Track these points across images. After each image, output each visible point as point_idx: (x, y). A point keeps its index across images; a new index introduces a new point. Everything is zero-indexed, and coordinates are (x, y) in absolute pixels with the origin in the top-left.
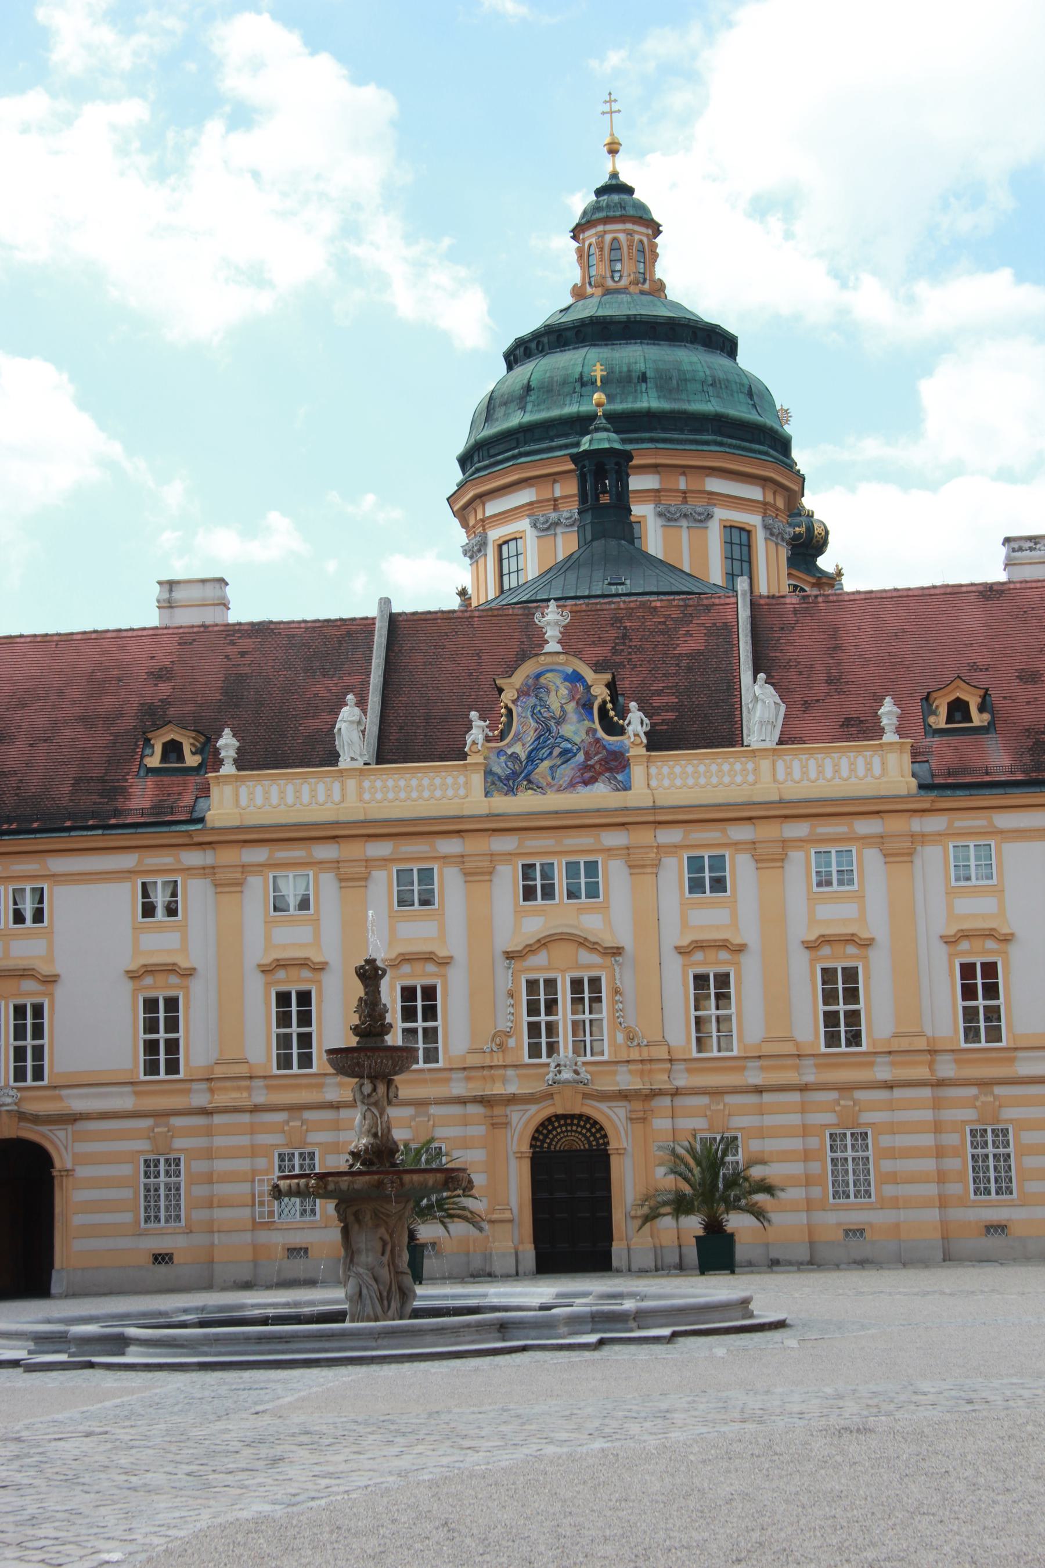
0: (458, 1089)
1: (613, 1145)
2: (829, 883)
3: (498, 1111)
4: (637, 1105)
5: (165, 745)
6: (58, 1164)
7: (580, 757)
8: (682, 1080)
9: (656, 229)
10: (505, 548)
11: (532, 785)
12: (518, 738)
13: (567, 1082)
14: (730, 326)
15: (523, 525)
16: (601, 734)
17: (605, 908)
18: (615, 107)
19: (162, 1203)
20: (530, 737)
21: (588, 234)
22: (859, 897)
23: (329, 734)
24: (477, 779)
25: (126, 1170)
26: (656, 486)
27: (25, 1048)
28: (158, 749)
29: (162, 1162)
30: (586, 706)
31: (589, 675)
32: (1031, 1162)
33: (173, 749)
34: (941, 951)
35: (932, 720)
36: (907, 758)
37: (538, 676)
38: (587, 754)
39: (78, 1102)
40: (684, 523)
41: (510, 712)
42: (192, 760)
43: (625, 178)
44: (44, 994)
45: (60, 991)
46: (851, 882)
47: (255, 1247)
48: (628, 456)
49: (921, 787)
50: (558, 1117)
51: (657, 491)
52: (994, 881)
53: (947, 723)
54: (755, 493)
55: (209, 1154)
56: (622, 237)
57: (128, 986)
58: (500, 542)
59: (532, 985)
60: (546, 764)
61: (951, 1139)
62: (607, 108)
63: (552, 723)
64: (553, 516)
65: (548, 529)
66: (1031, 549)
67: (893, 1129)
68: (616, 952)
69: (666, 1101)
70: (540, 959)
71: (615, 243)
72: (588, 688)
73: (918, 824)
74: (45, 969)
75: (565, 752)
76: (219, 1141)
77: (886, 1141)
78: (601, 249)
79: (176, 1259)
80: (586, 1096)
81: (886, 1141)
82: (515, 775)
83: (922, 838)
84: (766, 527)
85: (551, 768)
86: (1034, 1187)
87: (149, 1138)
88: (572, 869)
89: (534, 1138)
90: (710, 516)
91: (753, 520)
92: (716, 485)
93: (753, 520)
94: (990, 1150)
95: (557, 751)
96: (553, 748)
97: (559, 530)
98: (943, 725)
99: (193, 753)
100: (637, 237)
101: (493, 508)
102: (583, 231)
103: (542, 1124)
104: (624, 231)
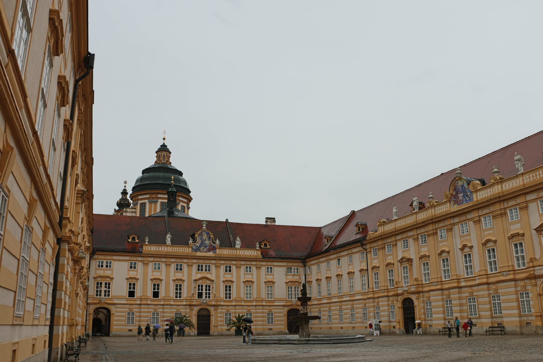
0: (184, 303)
1: (211, 314)
2: (247, 272)
3: (192, 307)
4: (216, 307)
5: (132, 237)
6: (112, 313)
7: (208, 247)
8: (222, 304)
9: (170, 153)
11: (200, 251)
12: (198, 243)
13: (205, 303)
15: (147, 201)
16: (212, 243)
17: (211, 273)
18: (165, 132)
19: (131, 320)
20: (200, 243)
22: (252, 274)
23: (165, 239)
24: (190, 249)
25: (124, 314)
27: (98, 290)
28: (131, 238)
29: (131, 313)
30: (209, 238)
31: (211, 233)
32: (276, 319)
33: (134, 239)
34: (264, 284)
35: (261, 246)
36: (260, 252)
37: (202, 232)
38: (209, 247)
39: (116, 302)
41: (196, 238)
42: (137, 241)
44: (136, 282)
45: (114, 281)
46: (251, 272)
47: (221, 329)
48: (176, 193)
49: (262, 257)
50: (202, 309)
52: (273, 273)
53: (264, 247)
54: (186, 201)
55: (163, 312)
56: (165, 154)
57: (126, 281)
59: (199, 286)
60: (202, 248)
61: (264, 315)
62: (164, 132)
63: (204, 241)
64: (153, 200)
66: (271, 220)
67: (256, 313)
68: (213, 281)
69: (220, 307)
70: (200, 281)
72: (210, 235)
73: (262, 263)
74: (111, 277)
75: (206, 246)
76: (142, 310)
77: (255, 315)
79: (133, 330)
80: (207, 305)
81: (255, 315)
82: (197, 249)
83: (262, 265)
85: (203, 248)
86: (276, 323)
87: (129, 309)
88: (206, 266)
89: (198, 312)
90: (180, 204)
91: (185, 205)
92: (180, 199)
93: (185, 205)
94: (270, 316)
95: (204, 246)
96: (203, 245)
97: (153, 203)
98: (263, 247)
99: (138, 239)
101: (140, 197)
103: (199, 310)
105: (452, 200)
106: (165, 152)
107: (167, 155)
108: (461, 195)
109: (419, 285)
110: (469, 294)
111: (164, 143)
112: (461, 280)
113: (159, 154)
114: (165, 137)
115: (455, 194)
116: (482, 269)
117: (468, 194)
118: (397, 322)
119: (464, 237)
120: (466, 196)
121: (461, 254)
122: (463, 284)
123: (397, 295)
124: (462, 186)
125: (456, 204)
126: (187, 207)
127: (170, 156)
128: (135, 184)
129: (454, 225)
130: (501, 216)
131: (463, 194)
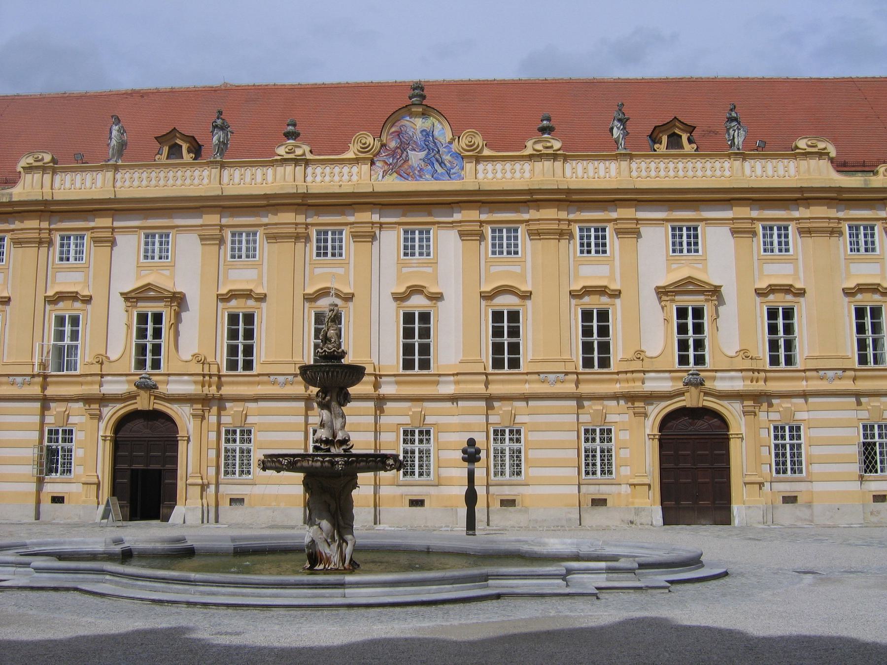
105: (381, 159)
108: (416, 157)
109: (210, 376)
110: (233, 419)
112: (384, 379)
115: (397, 148)
116: (551, 358)
117: (444, 157)
118: (83, 484)
119: (415, 265)
120: (437, 161)
121: (395, 308)
122: (387, 390)
123: (104, 400)
124: (427, 134)
125: (395, 175)
129: (381, 228)
130: (558, 237)
131: (425, 153)
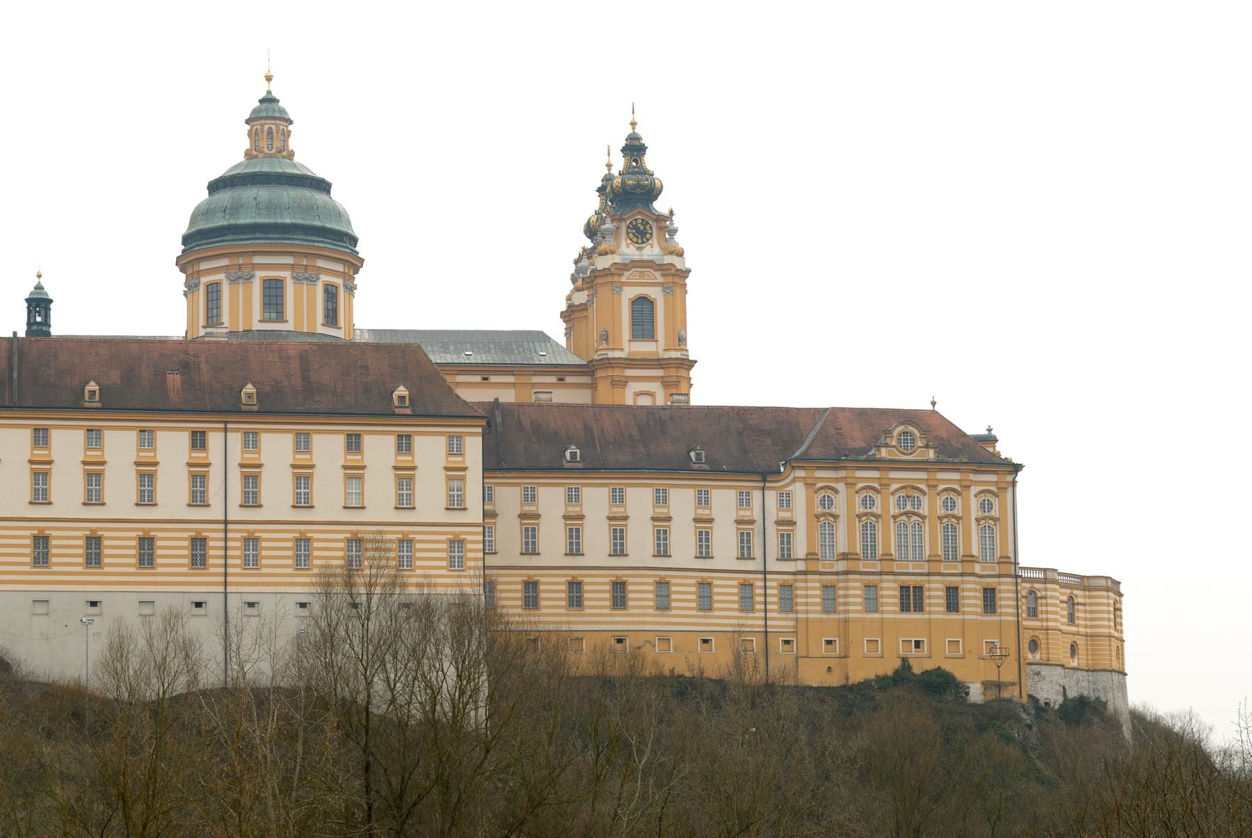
10: (210, 287)
14: (328, 178)
21: (255, 123)
26: (292, 262)
40: (305, 282)
43: (275, 94)
51: (292, 265)
54: (340, 268)
56: (274, 127)
58: (208, 284)
64: (239, 274)
65: (236, 280)
71: (270, 132)
78: (262, 132)
84: (344, 285)
91: (339, 281)
92: (321, 263)
93: (339, 281)
97: (241, 282)
100: (281, 127)
101: (204, 266)
102: (253, 122)
104: (275, 124)
106: (274, 122)
107: (278, 131)
111: (269, 92)
113: (254, 128)
114: (272, 73)
126: (345, 286)
127: (289, 132)
128: (188, 229)
